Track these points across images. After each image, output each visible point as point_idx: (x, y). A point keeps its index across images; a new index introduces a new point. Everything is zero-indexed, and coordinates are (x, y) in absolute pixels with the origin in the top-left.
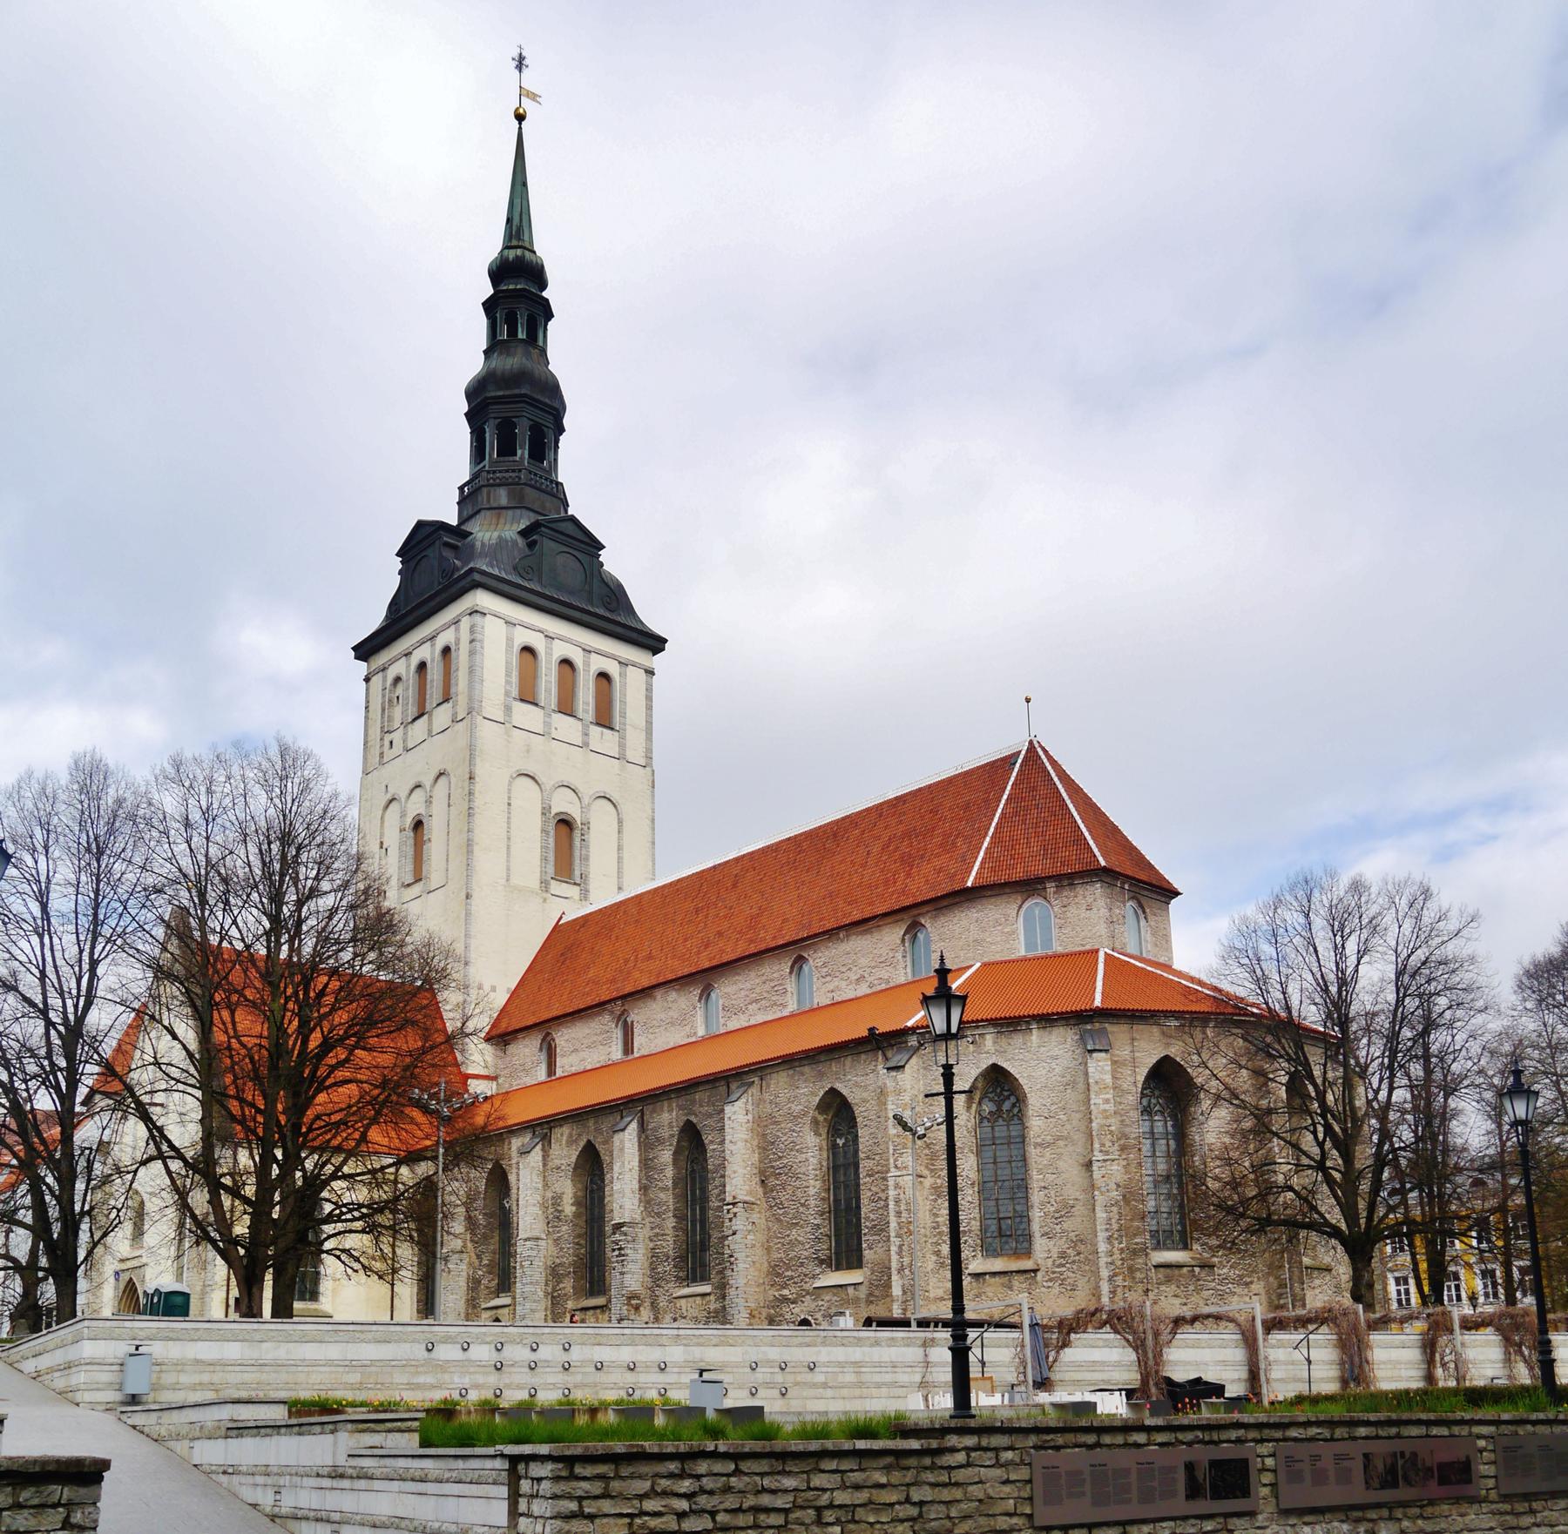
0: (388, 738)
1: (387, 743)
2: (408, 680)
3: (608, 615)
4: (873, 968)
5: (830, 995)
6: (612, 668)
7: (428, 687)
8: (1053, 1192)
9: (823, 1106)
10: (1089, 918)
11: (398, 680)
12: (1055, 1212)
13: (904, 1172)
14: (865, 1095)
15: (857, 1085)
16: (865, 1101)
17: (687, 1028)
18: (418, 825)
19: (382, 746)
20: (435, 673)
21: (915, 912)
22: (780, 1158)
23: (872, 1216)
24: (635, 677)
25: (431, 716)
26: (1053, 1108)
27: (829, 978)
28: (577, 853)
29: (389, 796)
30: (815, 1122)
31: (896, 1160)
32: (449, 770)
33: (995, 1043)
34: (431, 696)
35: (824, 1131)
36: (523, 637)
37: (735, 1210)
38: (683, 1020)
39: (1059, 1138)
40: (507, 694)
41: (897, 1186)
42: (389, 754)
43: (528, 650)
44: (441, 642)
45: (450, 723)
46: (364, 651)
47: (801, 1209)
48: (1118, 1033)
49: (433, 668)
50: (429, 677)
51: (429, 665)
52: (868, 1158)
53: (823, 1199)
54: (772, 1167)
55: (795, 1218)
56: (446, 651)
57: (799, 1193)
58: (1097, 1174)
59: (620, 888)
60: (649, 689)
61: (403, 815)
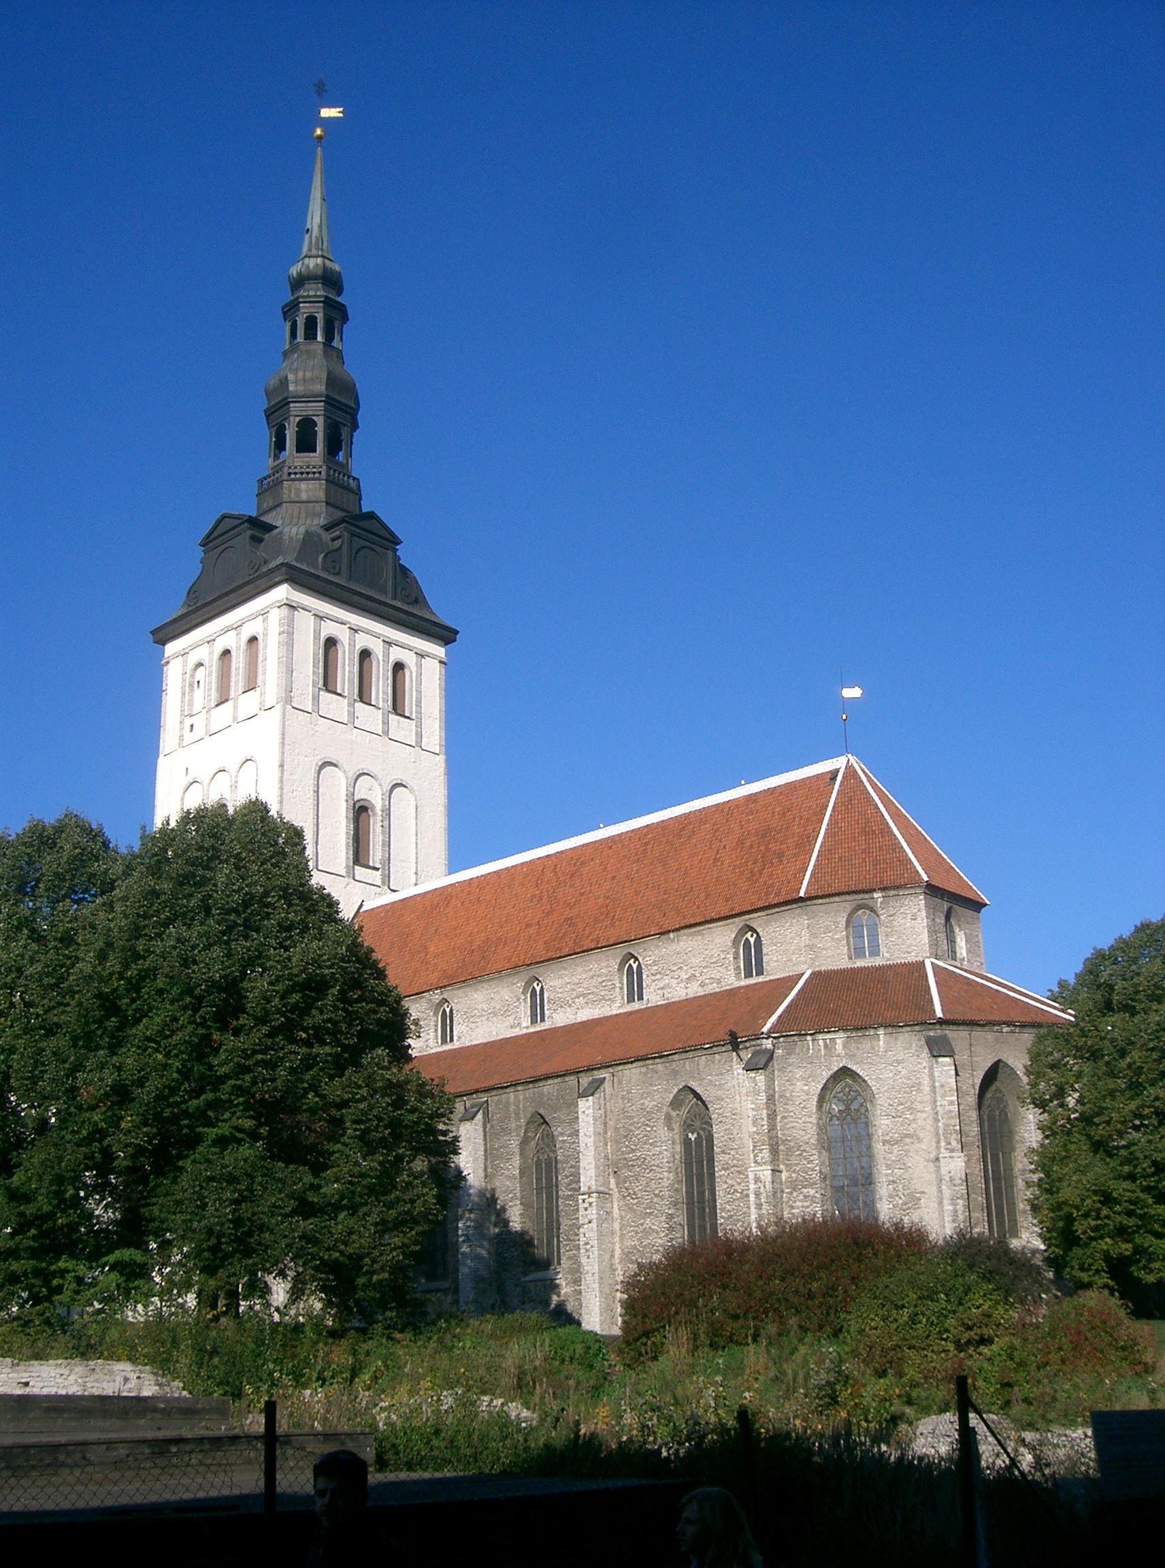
0: (188, 721)
1: (187, 728)
3: (405, 607)
4: (705, 967)
5: (659, 992)
6: (409, 659)
7: (233, 674)
8: (900, 1186)
9: (676, 1103)
10: (913, 928)
12: (905, 1204)
13: (764, 1167)
14: (719, 1093)
15: (711, 1083)
16: (720, 1099)
17: (511, 1019)
20: (238, 662)
21: (747, 917)
22: (633, 1151)
23: (728, 1207)
25: (236, 699)
26: (900, 1108)
27: (658, 976)
29: (190, 779)
30: (668, 1118)
31: (755, 1156)
33: (845, 1046)
35: (676, 1126)
36: (329, 629)
37: (591, 1200)
39: (907, 1136)
40: (314, 684)
41: (757, 1180)
43: (331, 643)
44: (247, 632)
47: (655, 1200)
48: (958, 1036)
50: (234, 665)
51: (234, 653)
52: (723, 1152)
53: (676, 1190)
54: (625, 1159)
55: (650, 1208)
56: (253, 640)
57: (652, 1184)
58: (944, 1171)
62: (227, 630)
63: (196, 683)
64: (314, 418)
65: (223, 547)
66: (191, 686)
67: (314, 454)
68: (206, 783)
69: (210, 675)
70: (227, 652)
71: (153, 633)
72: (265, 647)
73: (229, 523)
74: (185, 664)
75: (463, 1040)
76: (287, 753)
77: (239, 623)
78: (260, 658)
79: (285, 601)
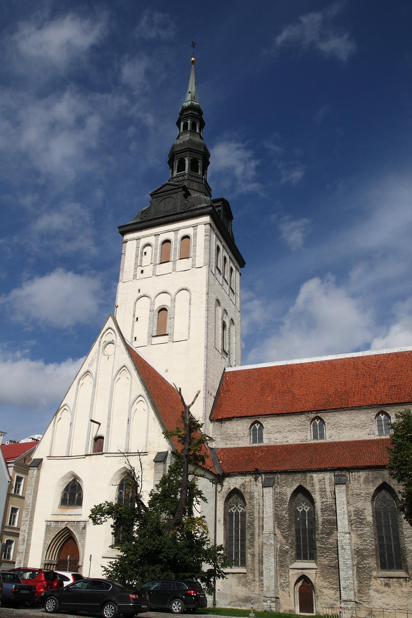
2: (156, 246)
11: (148, 245)
18: (163, 309)
19: (136, 271)
20: (176, 246)
25: (175, 262)
29: (141, 294)
32: (189, 287)
34: (175, 255)
38: (364, 426)
42: (139, 275)
49: (176, 244)
56: (186, 237)
61: (153, 304)
63: (144, 253)
64: (198, 160)
65: (165, 197)
66: (142, 253)
67: (197, 174)
69: (156, 249)
70: (167, 241)
72: (195, 241)
74: (138, 244)
75: (333, 438)
77: (178, 229)
78: (192, 244)
79: (209, 222)
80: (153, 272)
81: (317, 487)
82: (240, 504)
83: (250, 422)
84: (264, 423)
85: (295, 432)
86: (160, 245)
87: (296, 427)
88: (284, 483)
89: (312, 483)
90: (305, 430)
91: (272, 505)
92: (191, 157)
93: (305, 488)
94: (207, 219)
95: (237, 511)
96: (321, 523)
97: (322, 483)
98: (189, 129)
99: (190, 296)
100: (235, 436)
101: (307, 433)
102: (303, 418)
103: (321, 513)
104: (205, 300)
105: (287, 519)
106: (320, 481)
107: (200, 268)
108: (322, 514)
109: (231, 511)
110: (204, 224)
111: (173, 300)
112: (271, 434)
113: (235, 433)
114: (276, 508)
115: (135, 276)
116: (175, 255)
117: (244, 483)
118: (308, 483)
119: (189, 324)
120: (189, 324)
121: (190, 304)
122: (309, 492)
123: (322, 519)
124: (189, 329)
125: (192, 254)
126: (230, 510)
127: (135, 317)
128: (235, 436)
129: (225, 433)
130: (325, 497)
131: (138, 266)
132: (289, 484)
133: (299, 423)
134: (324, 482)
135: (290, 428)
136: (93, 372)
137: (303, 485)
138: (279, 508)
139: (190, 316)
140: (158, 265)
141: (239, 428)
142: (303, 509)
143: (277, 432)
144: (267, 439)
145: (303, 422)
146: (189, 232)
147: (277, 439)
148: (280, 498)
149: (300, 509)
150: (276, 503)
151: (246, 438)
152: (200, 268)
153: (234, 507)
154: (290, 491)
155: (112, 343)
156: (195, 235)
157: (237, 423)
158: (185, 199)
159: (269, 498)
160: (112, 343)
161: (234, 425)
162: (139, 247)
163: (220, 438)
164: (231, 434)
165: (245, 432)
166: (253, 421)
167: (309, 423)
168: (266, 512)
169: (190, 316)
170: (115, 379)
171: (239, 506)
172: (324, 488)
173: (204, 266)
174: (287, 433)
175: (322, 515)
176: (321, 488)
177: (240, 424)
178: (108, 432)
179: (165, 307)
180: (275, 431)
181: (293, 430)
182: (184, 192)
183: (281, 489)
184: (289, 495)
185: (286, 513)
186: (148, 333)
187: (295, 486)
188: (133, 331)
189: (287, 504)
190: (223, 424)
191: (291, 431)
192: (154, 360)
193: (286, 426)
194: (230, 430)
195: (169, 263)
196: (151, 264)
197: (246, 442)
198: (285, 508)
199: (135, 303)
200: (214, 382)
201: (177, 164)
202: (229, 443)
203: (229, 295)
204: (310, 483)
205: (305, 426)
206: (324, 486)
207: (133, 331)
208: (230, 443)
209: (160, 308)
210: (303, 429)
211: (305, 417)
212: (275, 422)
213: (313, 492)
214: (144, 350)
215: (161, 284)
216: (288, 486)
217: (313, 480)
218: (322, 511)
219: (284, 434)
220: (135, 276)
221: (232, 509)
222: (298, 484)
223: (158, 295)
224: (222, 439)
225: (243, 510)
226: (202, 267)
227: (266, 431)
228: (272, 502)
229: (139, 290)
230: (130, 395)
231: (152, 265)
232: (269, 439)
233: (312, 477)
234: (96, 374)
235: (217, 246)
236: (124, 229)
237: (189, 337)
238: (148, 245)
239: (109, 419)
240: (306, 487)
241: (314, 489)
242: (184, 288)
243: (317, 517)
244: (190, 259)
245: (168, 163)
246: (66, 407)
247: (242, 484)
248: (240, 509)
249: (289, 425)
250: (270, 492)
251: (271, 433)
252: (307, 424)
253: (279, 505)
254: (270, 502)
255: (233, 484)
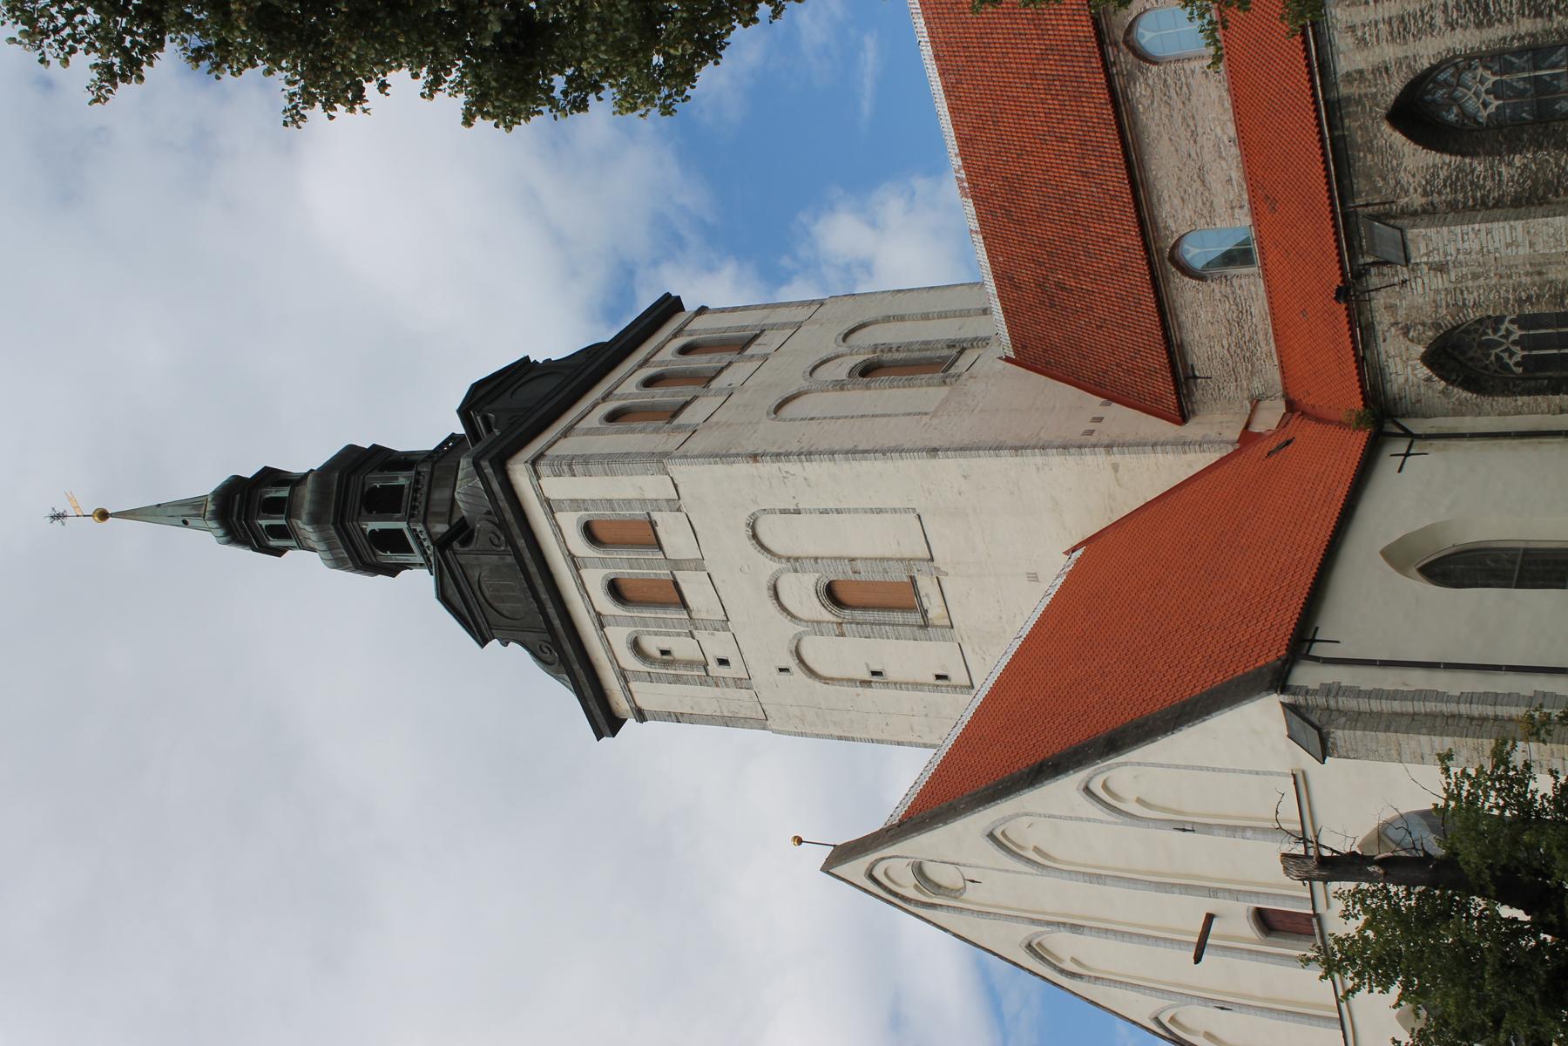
0: (714, 668)
1: (723, 671)
11: (636, 647)
18: (832, 595)
24: (700, 323)
25: (677, 564)
28: (916, 355)
29: (792, 663)
44: (580, 546)
45: (682, 516)
46: (606, 721)
51: (612, 572)
56: (589, 532)
59: (985, 311)
60: (723, 310)
62: (582, 586)
63: (664, 657)
64: (366, 489)
66: (666, 664)
67: (406, 491)
68: (800, 628)
70: (615, 589)
71: (599, 736)
73: (452, 591)
76: (739, 450)
77: (569, 559)
80: (718, 631)
81: (1390, 52)
82: (1487, 334)
83: (1177, 280)
84: (1174, 229)
85: (1197, 117)
86: (630, 612)
87: (1175, 114)
88: (1384, 179)
89: (1373, 73)
90: (1183, 79)
91: (1477, 226)
92: (359, 514)
93: (1397, 100)
94: (520, 473)
95: (1515, 343)
96: (1539, 20)
97: (1370, 35)
98: (283, 522)
99: (772, 511)
100: (1236, 330)
101: (1193, 72)
102: (1140, 93)
103: (1496, 24)
104: (776, 465)
105: (1534, 159)
106: (1362, 43)
107: (675, 486)
108: (1500, 21)
109: (1517, 364)
110: (539, 478)
111: (795, 562)
112: (1212, 202)
113: (1224, 331)
114: (1491, 204)
115: (738, 683)
116: (650, 564)
117: (1402, 329)
118: (1374, 90)
119: (865, 511)
120: (865, 511)
121: (798, 512)
122: (1412, 81)
123: (1520, 19)
124: (880, 511)
125: (639, 513)
126: (1515, 369)
127: (869, 679)
128: (1236, 330)
129: (1228, 365)
130: (1427, 18)
131: (708, 675)
132: (1385, 162)
133: (1160, 106)
134: (1364, 25)
135: (1182, 137)
136: (1025, 931)
137: (1386, 108)
138: (1489, 191)
139: (838, 511)
140: (694, 616)
141: (1204, 316)
142: (1487, 92)
143: (1203, 182)
144: (1233, 215)
145: (1152, 91)
146: (570, 523)
147: (1230, 180)
148: (1448, 190)
149: (1485, 105)
150: (1470, 203)
151: (1238, 291)
152: (675, 486)
153: (1501, 354)
154: (1417, 155)
155: (919, 870)
156: (576, 504)
157: (1188, 325)
158: (475, 539)
159: (1449, 241)
160: (919, 870)
161: (1197, 336)
162: (649, 673)
163: (1250, 379)
164: (1230, 345)
165: (1218, 296)
166: (1174, 270)
167: (1154, 68)
168: (1508, 245)
169: (838, 511)
170: (1040, 862)
171: (1496, 337)
172: (1390, 24)
173: (667, 474)
174: (1202, 147)
175: (1504, 20)
176: (1389, 38)
177: (1190, 316)
178: (1235, 894)
179: (822, 585)
180: (1201, 189)
181: (1188, 126)
182: (456, 545)
183: (1412, 190)
184: (1433, 158)
185: (1510, 164)
186: (915, 639)
187: (1393, 138)
188: (917, 686)
189: (1471, 165)
190: (1197, 373)
191: (1192, 131)
192: (1001, 618)
193: (1177, 151)
194: (1218, 348)
195: (679, 581)
196: (693, 638)
197: (1252, 288)
198: (1486, 171)
199: (826, 680)
200: (1054, 407)
201: (389, 553)
202: (1265, 349)
203: (765, 358)
204: (1376, 80)
205: (1169, 81)
206: (1381, 26)
207: (917, 686)
208: (1263, 344)
209: (827, 602)
210: (1181, 88)
211: (1135, 84)
212: (1166, 191)
213: (1409, 66)
214: (973, 650)
215: (748, 604)
216: (1395, 163)
217: (1361, 72)
218: (1489, 21)
219: (1207, 157)
220: (738, 683)
221: (1511, 363)
222: (1386, 127)
223: (789, 613)
224: (1252, 374)
225: (1512, 322)
226: (672, 478)
227: (1203, 221)
228: (1465, 227)
229: (781, 670)
230: (1089, 820)
231: (695, 633)
232: (1232, 208)
233: (1348, 74)
234: (1033, 922)
235: (606, 425)
236: (601, 720)
237: (907, 510)
238: (636, 647)
239: (1187, 889)
240: (1393, 97)
241: (1399, 62)
242: (751, 533)
243: (1513, 38)
244: (656, 516)
245: (394, 576)
246: (1165, 1019)
247: (1406, 334)
248: (1509, 333)
249: (1170, 140)
250: (1424, 236)
251: (1208, 204)
252: (1159, 76)
253: (1479, 194)
254: (1467, 234)
255: (1409, 368)
